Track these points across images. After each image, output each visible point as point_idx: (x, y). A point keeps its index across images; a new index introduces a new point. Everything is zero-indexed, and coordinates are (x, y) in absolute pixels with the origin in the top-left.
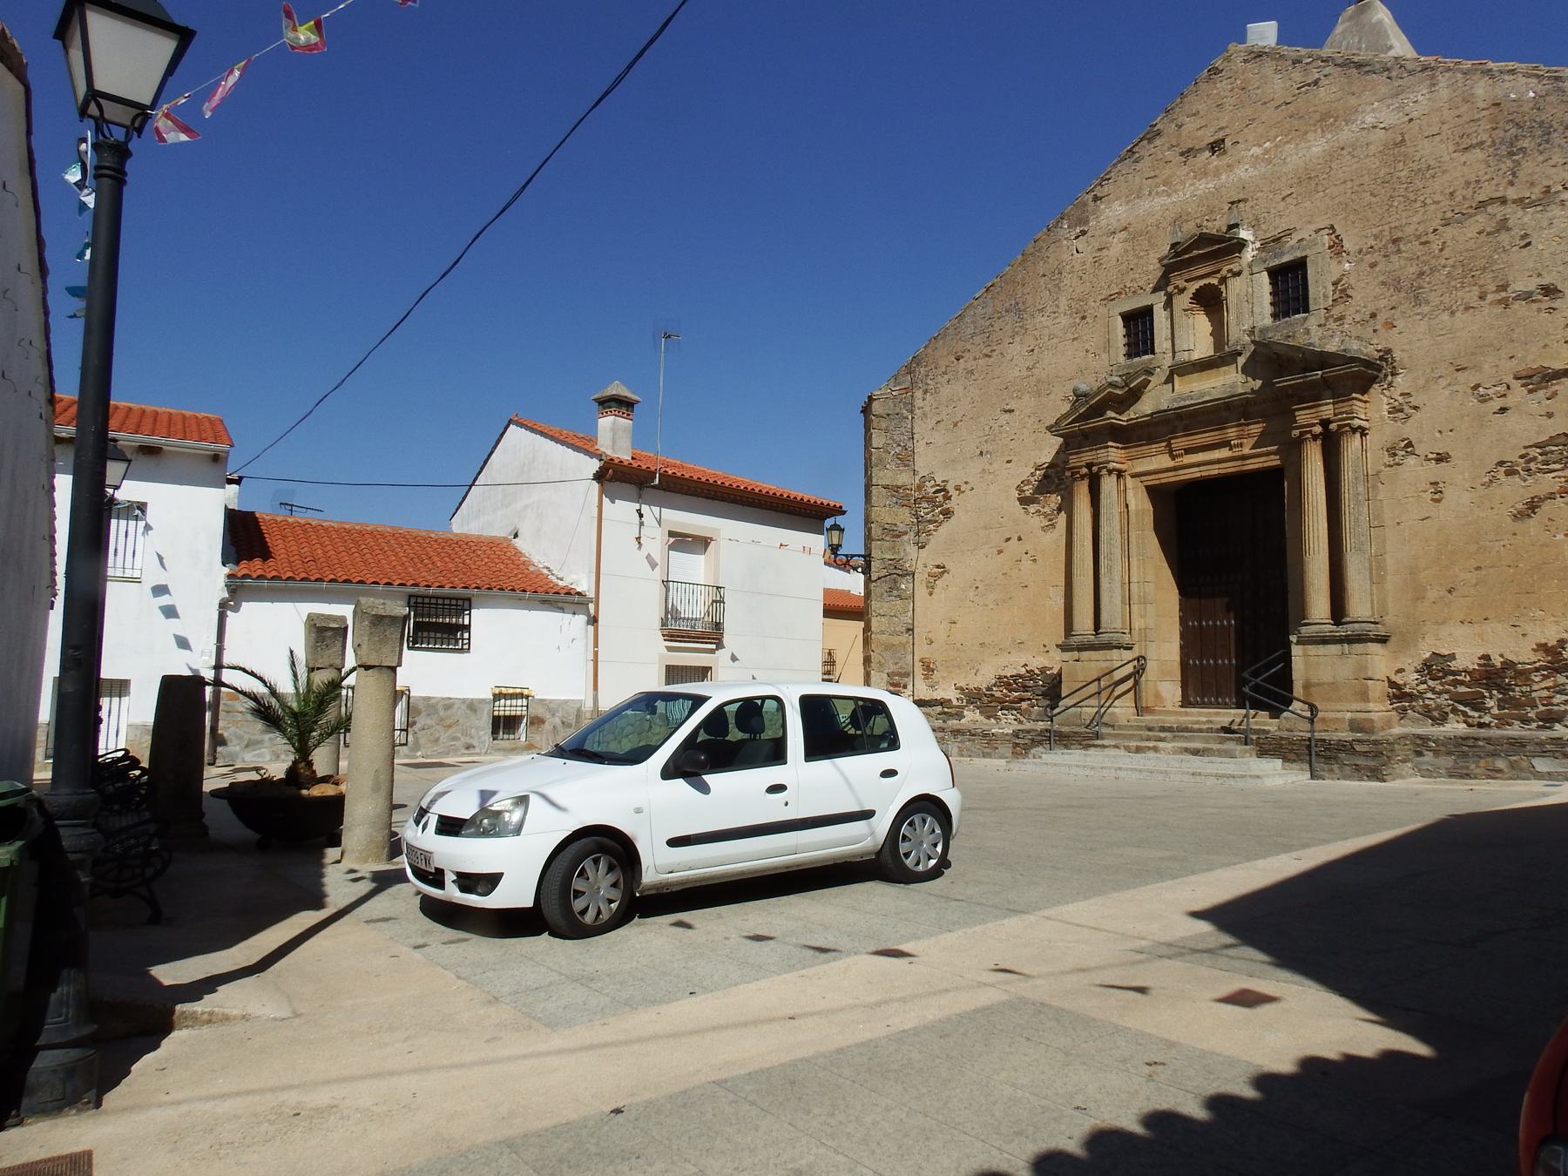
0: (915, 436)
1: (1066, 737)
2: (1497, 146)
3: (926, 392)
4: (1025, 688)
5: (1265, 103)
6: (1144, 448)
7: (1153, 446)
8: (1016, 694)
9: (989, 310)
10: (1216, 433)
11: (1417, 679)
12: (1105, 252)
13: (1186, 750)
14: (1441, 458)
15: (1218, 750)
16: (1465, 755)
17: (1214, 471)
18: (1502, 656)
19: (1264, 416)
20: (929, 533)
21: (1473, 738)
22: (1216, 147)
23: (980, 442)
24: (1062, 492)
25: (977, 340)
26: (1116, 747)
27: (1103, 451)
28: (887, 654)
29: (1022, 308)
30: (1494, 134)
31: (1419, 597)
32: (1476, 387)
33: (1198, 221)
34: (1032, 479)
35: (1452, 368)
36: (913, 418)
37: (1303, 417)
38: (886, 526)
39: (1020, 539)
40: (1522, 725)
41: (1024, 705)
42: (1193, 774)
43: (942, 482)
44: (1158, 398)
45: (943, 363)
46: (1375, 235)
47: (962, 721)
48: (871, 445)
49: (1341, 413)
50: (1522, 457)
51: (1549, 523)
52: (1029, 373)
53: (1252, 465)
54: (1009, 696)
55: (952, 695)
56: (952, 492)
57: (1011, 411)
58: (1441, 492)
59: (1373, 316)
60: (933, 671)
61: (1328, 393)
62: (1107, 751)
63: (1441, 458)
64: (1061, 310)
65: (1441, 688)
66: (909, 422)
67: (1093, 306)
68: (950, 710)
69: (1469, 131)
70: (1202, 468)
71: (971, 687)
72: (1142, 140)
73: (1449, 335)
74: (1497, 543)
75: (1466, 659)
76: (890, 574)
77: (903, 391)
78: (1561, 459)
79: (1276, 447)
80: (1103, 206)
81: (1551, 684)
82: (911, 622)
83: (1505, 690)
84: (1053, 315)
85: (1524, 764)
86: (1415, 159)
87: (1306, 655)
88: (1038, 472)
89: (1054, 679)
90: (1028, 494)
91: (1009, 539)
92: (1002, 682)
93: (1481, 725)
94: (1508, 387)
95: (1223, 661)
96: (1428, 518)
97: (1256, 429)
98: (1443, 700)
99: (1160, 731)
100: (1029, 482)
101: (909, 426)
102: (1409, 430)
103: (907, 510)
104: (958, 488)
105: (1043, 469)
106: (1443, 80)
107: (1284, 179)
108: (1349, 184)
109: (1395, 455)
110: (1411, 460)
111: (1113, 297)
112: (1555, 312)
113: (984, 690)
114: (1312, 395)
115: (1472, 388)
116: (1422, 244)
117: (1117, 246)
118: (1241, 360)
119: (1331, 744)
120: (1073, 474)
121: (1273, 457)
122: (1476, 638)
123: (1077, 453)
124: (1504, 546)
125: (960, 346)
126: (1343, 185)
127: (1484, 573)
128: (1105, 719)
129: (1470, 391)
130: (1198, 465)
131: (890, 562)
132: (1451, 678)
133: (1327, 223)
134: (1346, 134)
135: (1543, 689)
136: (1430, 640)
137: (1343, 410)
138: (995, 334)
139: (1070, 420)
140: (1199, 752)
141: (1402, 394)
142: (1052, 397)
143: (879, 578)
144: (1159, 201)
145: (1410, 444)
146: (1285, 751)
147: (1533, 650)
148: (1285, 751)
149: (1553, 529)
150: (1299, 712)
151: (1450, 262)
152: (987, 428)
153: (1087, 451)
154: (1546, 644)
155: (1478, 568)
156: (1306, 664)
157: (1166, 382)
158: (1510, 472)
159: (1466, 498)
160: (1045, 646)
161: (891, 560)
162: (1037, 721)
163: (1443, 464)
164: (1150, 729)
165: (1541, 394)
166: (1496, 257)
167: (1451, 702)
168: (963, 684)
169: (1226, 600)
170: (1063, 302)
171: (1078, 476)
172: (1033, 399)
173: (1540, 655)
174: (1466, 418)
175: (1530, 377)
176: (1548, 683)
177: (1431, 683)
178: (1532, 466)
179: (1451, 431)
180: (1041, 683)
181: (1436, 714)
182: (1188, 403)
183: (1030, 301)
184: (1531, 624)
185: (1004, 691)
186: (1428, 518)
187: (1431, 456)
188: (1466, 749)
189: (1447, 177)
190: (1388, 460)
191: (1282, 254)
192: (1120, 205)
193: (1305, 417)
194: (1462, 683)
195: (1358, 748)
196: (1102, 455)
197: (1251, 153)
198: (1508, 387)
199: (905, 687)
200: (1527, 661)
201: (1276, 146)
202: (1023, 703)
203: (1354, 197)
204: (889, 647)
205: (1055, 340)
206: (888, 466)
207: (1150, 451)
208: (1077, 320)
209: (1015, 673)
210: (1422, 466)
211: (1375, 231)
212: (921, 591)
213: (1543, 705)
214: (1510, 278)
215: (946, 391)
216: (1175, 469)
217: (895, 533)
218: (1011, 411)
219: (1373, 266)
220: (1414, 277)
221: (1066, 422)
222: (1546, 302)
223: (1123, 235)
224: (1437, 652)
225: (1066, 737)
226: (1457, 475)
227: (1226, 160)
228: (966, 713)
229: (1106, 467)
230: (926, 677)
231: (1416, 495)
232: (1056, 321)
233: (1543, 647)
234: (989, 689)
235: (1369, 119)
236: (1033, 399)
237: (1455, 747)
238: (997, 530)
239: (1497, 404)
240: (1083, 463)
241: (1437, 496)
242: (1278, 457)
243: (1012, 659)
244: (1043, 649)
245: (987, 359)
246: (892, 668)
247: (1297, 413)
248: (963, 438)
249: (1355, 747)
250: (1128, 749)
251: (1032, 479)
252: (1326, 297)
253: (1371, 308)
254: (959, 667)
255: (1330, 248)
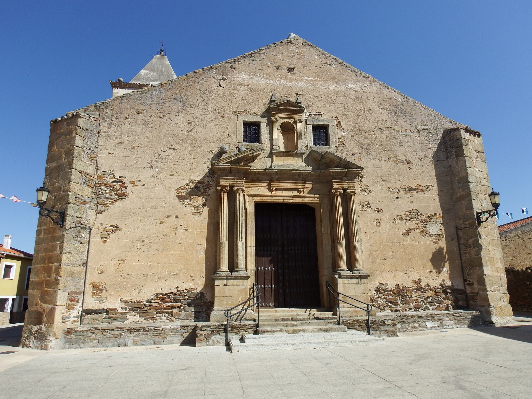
0: (99, 147)
1: (236, 328)
2: (391, 111)
3: (111, 124)
4: (176, 301)
5: (311, 63)
6: (255, 184)
7: (260, 184)
8: (169, 304)
9: (163, 95)
10: (293, 184)
11: (375, 294)
12: (236, 92)
13: (321, 330)
14: (379, 211)
15: (337, 329)
16: (404, 323)
17: (290, 200)
18: (402, 284)
19: (312, 181)
20: (106, 205)
21: (407, 316)
22: (291, 70)
23: (152, 161)
24: (206, 197)
25: (154, 107)
26: (281, 331)
27: (240, 181)
28: (70, 279)
29: (185, 101)
30: (390, 107)
31: (374, 262)
32: (389, 188)
33: (282, 96)
34: (187, 187)
35: (381, 180)
36: (98, 136)
37: (336, 185)
38: (78, 196)
39: (177, 217)
40: (409, 310)
41: (175, 310)
42: (351, 342)
43: (120, 177)
44: (259, 164)
45: (126, 113)
46: (353, 126)
47: (126, 322)
48: (75, 143)
49: (350, 187)
50: (404, 215)
51: (413, 238)
52: (188, 133)
53: (307, 201)
54: (163, 306)
55: (117, 305)
56: (127, 183)
57: (175, 149)
58: (379, 223)
59: (354, 154)
60: (102, 290)
61: (345, 178)
62: (276, 334)
63: (379, 211)
64: (210, 109)
65: (384, 297)
66: (96, 137)
67: (228, 113)
68: (114, 316)
69: (383, 103)
70: (293, 199)
71: (135, 300)
72: (256, 53)
73: (380, 168)
74: (399, 243)
75: (391, 286)
76: (77, 227)
77: (95, 119)
78: (416, 217)
79: (319, 195)
80: (235, 72)
81: (418, 295)
82: (86, 258)
83: (403, 297)
84: (204, 110)
85: (423, 325)
86: (366, 105)
87: (344, 284)
88: (191, 184)
89: (196, 296)
90: (183, 194)
91: (170, 216)
92: (159, 297)
93: (396, 311)
94: (399, 190)
95: (268, 286)
96: (375, 232)
97: (309, 186)
98: (384, 302)
99: (282, 321)
100: (184, 188)
101: (96, 140)
102: (368, 198)
103: (90, 189)
104: (133, 183)
105: (194, 183)
106: (374, 84)
107: (319, 93)
108: (343, 105)
109: (363, 207)
110: (369, 209)
111: (239, 112)
112: (411, 169)
113: (145, 302)
114: (340, 178)
115: (388, 188)
116: (369, 134)
117: (242, 91)
118: (304, 156)
119: (376, 322)
120: (222, 188)
121: (316, 199)
122: (394, 278)
123: (225, 179)
124: (401, 245)
125: (140, 107)
126: (341, 105)
127: (395, 254)
128: (245, 317)
129: (387, 189)
130: (283, 196)
131: (78, 219)
132: (387, 293)
133: (335, 116)
134: (342, 87)
135: (415, 296)
136: (379, 278)
137: (351, 186)
138: (166, 108)
139: (226, 162)
140: (327, 330)
141: (365, 185)
142: (202, 148)
143: (71, 228)
144: (264, 81)
145: (369, 204)
146: (356, 326)
147: (412, 282)
148: (356, 326)
149: (415, 240)
150: (362, 308)
151: (378, 143)
152: (157, 155)
153: (231, 179)
154: (415, 280)
155: (393, 252)
156: (344, 287)
157: (268, 157)
158: (401, 219)
159: (388, 226)
160: (191, 277)
161: (78, 217)
162: (184, 319)
163: (380, 213)
164: (276, 320)
165: (408, 195)
166: (392, 146)
167: (387, 302)
168: (128, 299)
169: (270, 258)
170: (211, 106)
171: (224, 190)
172: (190, 146)
173: (414, 284)
174: (387, 198)
175: (405, 188)
176: (417, 294)
177: (379, 295)
178: (407, 218)
179: (382, 202)
180: (187, 297)
181: (382, 307)
182: (281, 168)
183: (190, 99)
184: (411, 273)
185: (160, 302)
186: (375, 232)
187: (376, 209)
188: (404, 320)
189: (376, 115)
190: (361, 208)
191: (319, 121)
192: (245, 75)
193: (337, 185)
194: (390, 295)
195: (387, 323)
196: (239, 182)
197: (305, 79)
198: (399, 190)
199: (78, 301)
200: (410, 286)
201: (315, 80)
202: (174, 310)
203: (345, 110)
204: (71, 274)
205: (205, 122)
206: (83, 159)
207: (258, 186)
208: (219, 117)
209: (169, 291)
210: (373, 212)
211: (353, 125)
212: (96, 240)
213: (416, 302)
214: (397, 154)
215: (126, 128)
216: (271, 196)
217: (82, 201)
218: (175, 149)
219: (353, 136)
220: (367, 145)
221: (225, 162)
222: (408, 166)
223: (246, 88)
224: (382, 283)
225: (236, 328)
226: (385, 217)
227: (294, 77)
228: (129, 317)
229: (241, 189)
230: (95, 295)
231: (371, 223)
232: (206, 113)
233: (414, 282)
234: (149, 301)
235: (350, 86)
236: (190, 146)
237: (401, 319)
238: (161, 210)
239: (396, 195)
240: (228, 184)
241: (378, 224)
242: (319, 199)
243: (167, 283)
244: (190, 278)
245: (160, 119)
246: (72, 288)
247: (334, 183)
248: (138, 156)
249: (385, 322)
250: (288, 332)
251: (187, 187)
252: (336, 142)
253: (353, 151)
254: (125, 288)
255: (337, 125)
